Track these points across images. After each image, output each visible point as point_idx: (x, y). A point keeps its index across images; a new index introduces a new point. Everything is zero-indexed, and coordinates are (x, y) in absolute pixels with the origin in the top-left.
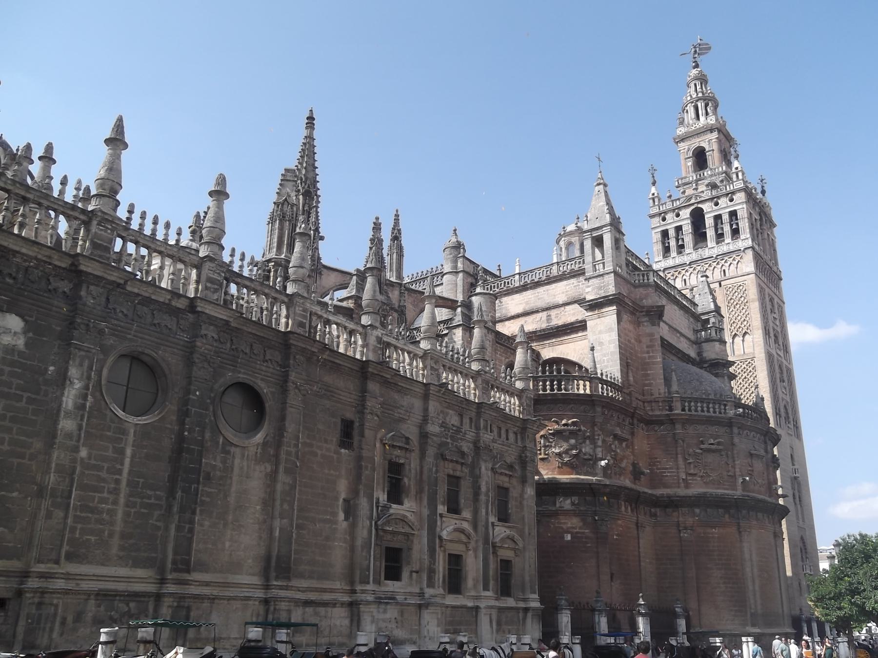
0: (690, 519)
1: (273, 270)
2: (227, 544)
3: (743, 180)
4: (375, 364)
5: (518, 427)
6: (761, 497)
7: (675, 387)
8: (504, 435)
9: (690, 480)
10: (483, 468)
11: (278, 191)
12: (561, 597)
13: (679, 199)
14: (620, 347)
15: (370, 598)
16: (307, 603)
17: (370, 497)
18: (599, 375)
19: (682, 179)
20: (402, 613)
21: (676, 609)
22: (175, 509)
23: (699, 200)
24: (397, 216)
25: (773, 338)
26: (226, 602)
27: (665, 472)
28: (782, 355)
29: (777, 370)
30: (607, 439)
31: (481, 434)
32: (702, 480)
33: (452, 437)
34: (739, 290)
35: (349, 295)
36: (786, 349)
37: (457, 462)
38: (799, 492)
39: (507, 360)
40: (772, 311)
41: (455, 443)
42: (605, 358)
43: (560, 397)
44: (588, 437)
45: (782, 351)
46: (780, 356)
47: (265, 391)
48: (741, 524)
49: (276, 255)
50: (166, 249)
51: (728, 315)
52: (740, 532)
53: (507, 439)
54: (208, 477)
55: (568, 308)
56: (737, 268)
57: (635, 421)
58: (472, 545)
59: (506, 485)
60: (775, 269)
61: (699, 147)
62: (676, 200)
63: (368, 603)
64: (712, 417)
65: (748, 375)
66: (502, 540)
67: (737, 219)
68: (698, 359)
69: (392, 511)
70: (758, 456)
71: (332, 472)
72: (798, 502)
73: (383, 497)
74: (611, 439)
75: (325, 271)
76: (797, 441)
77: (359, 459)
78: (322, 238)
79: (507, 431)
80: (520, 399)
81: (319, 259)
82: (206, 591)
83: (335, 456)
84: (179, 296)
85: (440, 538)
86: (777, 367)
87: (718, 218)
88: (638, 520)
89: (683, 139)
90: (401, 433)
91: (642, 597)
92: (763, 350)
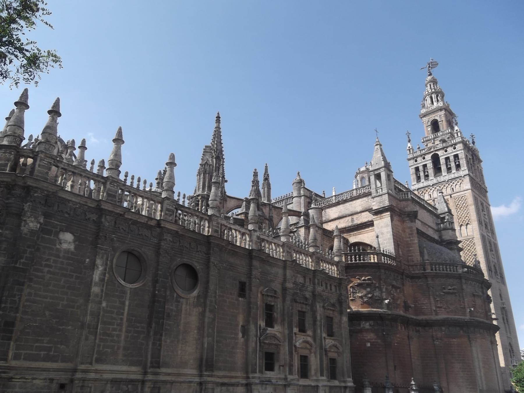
1: (200, 200)
2: (179, 352)
3: (461, 136)
4: (256, 251)
5: (337, 283)
6: (482, 320)
7: (426, 257)
8: (329, 287)
9: (438, 310)
10: (318, 306)
11: (202, 158)
12: (365, 380)
13: (424, 149)
14: (393, 235)
15: (257, 381)
16: (223, 384)
17: (256, 324)
18: (382, 252)
19: (425, 138)
20: (275, 390)
21: (435, 387)
22: (152, 333)
23: (436, 149)
24: (266, 167)
25: (484, 226)
26: (179, 384)
27: (423, 306)
28: (491, 236)
29: (488, 245)
30: (388, 288)
31: (316, 288)
33: (300, 290)
34: (462, 199)
35: (242, 212)
36: (493, 232)
37: (303, 303)
38: (506, 316)
39: (330, 244)
41: (302, 293)
42: (385, 242)
43: (361, 265)
44: (378, 287)
45: (490, 233)
46: (489, 236)
47: (198, 268)
48: (470, 336)
49: (202, 192)
50: (145, 194)
51: (456, 214)
52: (470, 341)
53: (331, 290)
54: (169, 316)
55: (363, 214)
56: (460, 186)
57: (404, 277)
58: (313, 350)
59: (331, 316)
60: (483, 186)
61: (434, 119)
62: (422, 150)
63: (256, 384)
64: (449, 274)
65: (470, 248)
66: (330, 347)
67: (458, 159)
68: (439, 240)
69: (268, 332)
70: (478, 296)
71: (235, 311)
72: (506, 322)
73: (263, 324)
74: (390, 287)
75: (228, 199)
76: (503, 285)
77: (249, 303)
78: (226, 181)
79: (331, 285)
80: (337, 267)
81: (225, 192)
82: (168, 378)
83: (236, 302)
84: (152, 219)
85: (295, 346)
86: (488, 243)
87: (447, 159)
88: (408, 334)
89: (425, 116)
90: (272, 288)
91: (413, 380)
92: (479, 233)
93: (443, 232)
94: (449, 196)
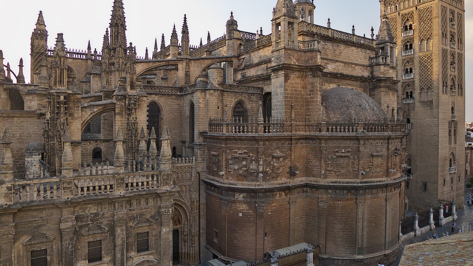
0: (325, 196)
9: (328, 173)
32: (335, 174)
40: (451, 20)
65: (428, 64)
93: (376, 68)
94: (415, 8)
